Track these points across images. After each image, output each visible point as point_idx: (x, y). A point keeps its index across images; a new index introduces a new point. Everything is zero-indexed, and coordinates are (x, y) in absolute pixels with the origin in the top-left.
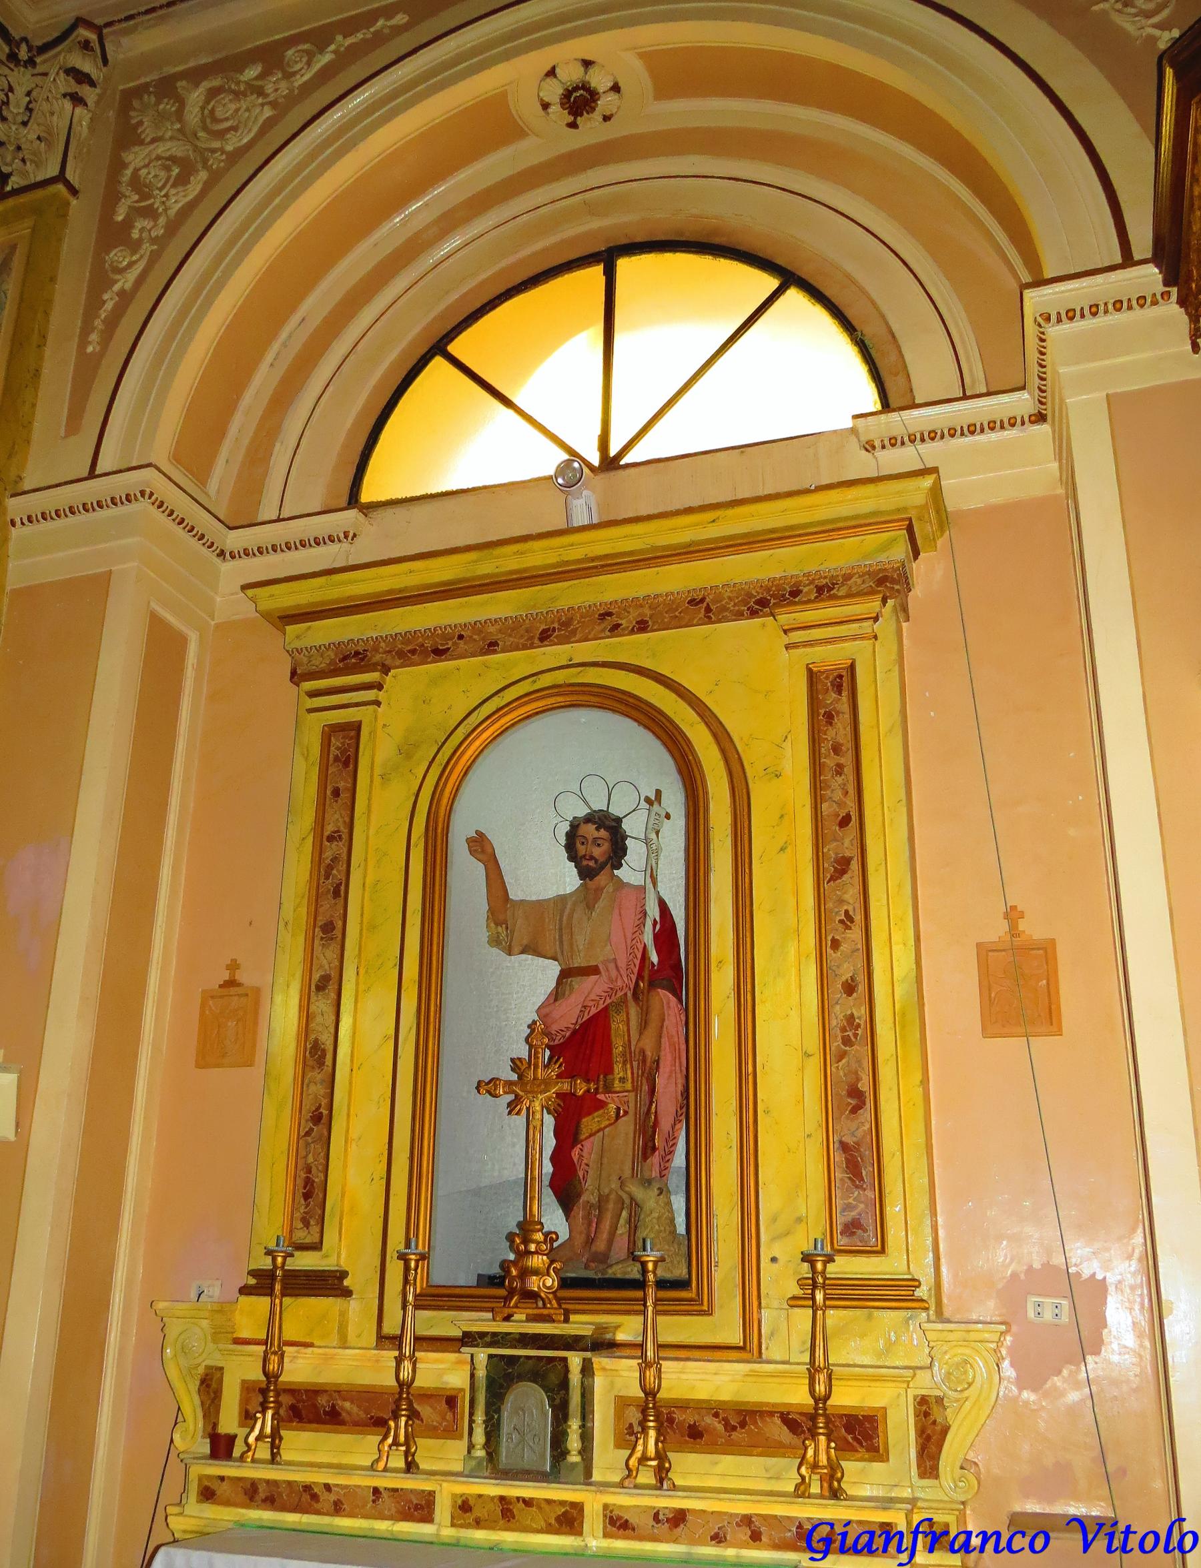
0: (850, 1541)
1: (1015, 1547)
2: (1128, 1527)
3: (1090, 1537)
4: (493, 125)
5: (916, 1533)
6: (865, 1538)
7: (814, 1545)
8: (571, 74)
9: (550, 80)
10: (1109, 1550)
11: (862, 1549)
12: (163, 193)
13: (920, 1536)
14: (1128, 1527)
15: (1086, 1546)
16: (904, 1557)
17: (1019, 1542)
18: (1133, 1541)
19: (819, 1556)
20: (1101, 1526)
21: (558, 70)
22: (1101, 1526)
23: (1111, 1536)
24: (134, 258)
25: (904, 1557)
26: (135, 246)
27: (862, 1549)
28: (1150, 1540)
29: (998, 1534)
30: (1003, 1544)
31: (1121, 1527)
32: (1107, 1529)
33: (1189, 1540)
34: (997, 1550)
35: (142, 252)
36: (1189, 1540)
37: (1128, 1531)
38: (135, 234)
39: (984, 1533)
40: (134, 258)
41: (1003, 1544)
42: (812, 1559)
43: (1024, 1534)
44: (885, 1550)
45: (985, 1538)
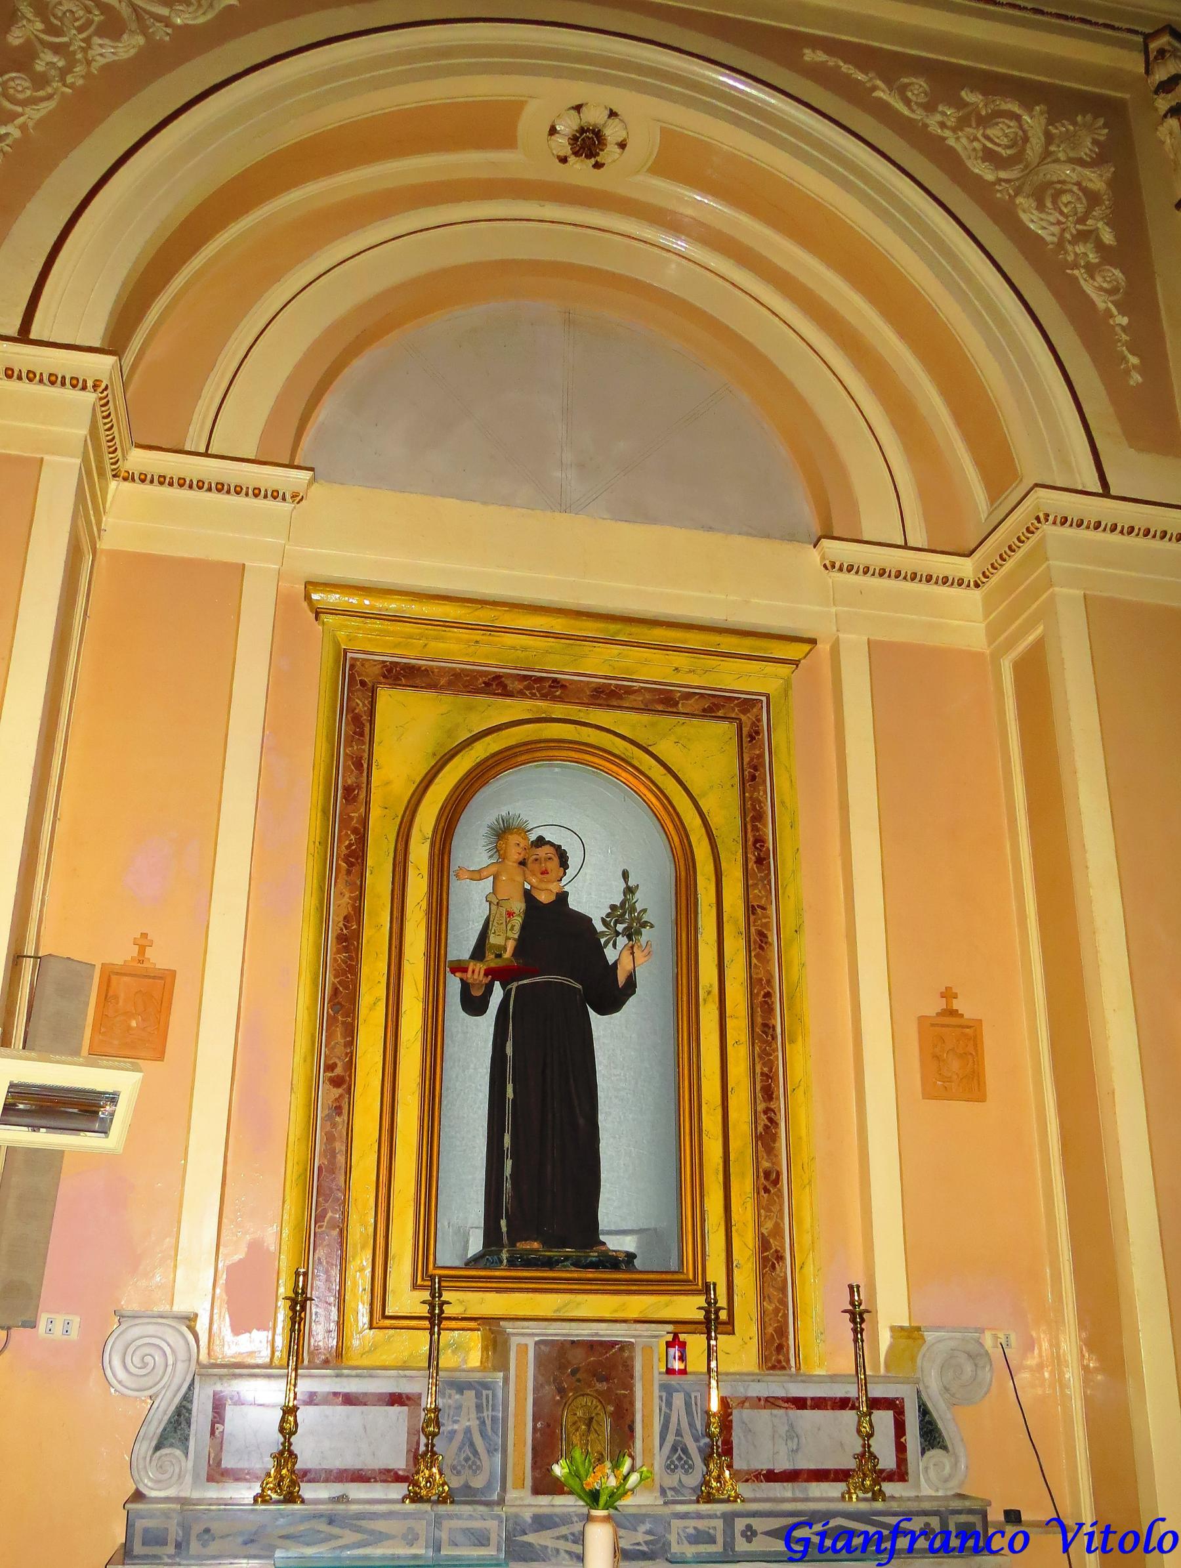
1: (994, 1547)
2: (1108, 1527)
3: (1070, 1536)
4: (493, 126)
10: (1089, 1551)
14: (1108, 1527)
18: (1113, 1541)
22: (1081, 1525)
24: (41, 93)
27: (841, 1549)
28: (1129, 1542)
32: (1087, 1529)
33: (1168, 1542)
35: (49, 90)
36: (1168, 1542)
38: (40, 67)
40: (41, 93)
43: (1003, 1534)
44: (864, 1550)
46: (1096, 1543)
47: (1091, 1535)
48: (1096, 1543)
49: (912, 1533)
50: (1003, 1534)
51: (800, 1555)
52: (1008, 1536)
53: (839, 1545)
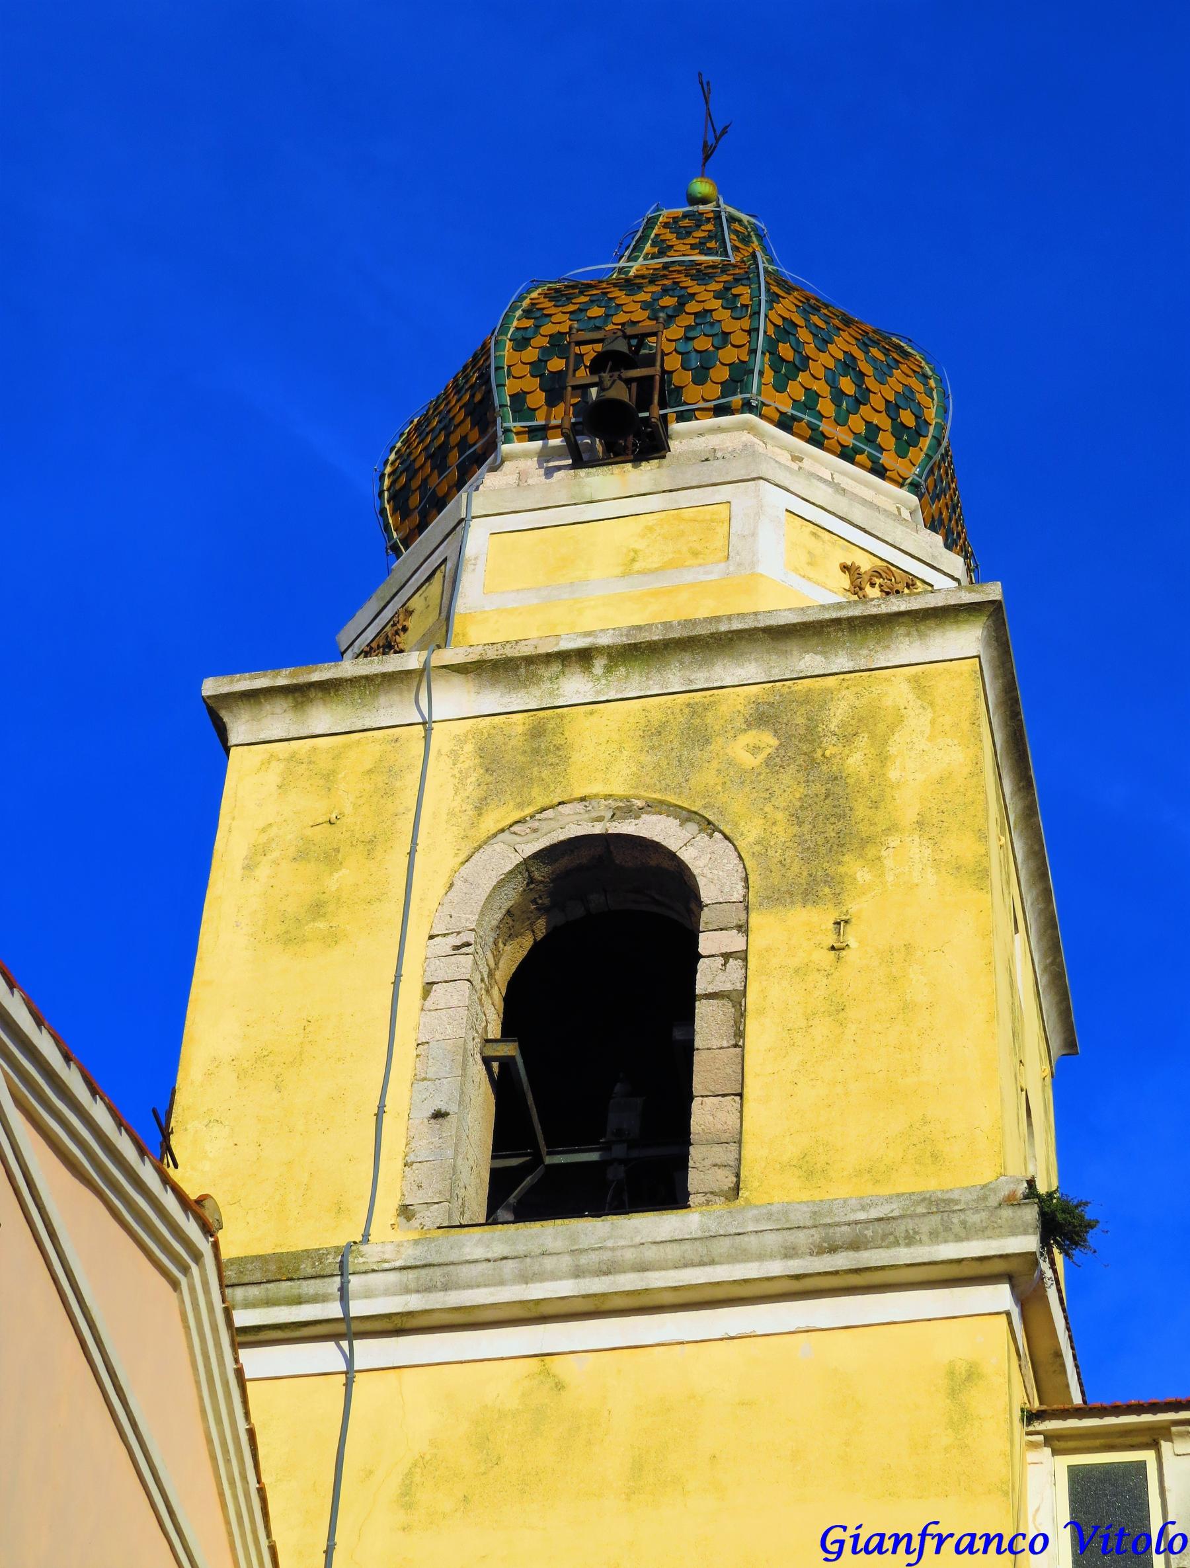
0: (861, 1545)
2: (1122, 1530)
3: (1086, 1540)
5: (923, 1535)
6: (876, 1540)
7: (829, 1547)
11: (873, 1551)
13: (928, 1538)
14: (1122, 1530)
16: (913, 1558)
19: (834, 1556)
20: (1096, 1528)
22: (1096, 1528)
23: (1106, 1538)
25: (913, 1558)
29: (1000, 1536)
30: (1005, 1545)
31: (1115, 1530)
33: (1178, 1543)
34: (999, 1551)
36: (1178, 1543)
37: (1121, 1534)
39: (987, 1535)
41: (1005, 1545)
42: (826, 1559)
45: (988, 1539)
46: (1112, 1543)
47: (1106, 1538)
48: (1112, 1543)
49: (940, 1535)
50: (1024, 1536)
51: (834, 1556)
52: (1029, 1538)
53: (871, 1546)
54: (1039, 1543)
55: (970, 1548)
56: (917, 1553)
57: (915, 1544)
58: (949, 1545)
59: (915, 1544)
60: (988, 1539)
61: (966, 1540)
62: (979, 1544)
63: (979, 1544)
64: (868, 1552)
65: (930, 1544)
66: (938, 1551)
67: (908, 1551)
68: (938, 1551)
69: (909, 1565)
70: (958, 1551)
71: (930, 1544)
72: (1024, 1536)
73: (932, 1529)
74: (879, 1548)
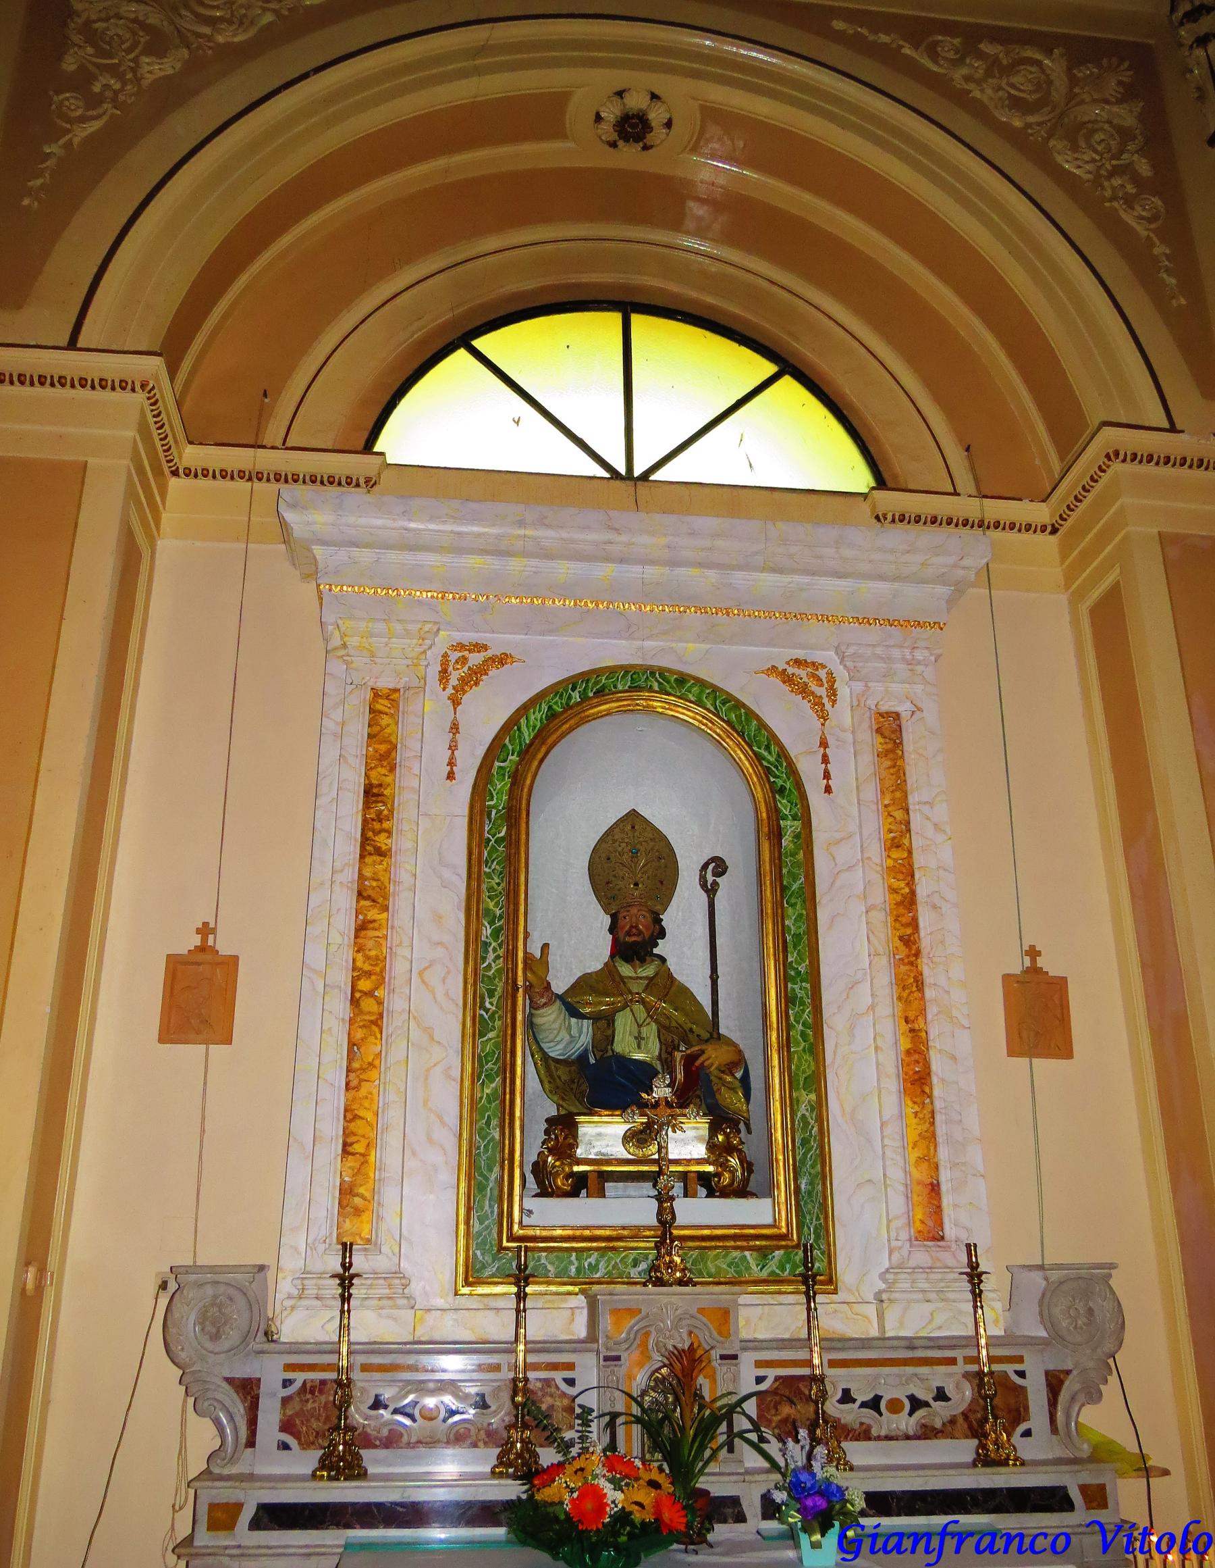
1: (1038, 1547)
3: (1109, 1538)
8: (637, 101)
9: (616, 99)
11: (891, 1551)
12: (132, 56)
13: (948, 1538)
15: (1106, 1547)
16: (932, 1558)
17: (1041, 1543)
19: (849, 1557)
21: (626, 95)
24: (90, 113)
25: (932, 1558)
26: (93, 101)
29: (1021, 1536)
34: (1020, 1551)
35: (100, 111)
40: (90, 113)
47: (1130, 1536)
54: (1061, 1541)
55: (991, 1548)
56: (936, 1553)
57: (935, 1543)
58: (970, 1543)
59: (935, 1543)
60: (1009, 1538)
61: (987, 1540)
62: (1000, 1543)
63: (1000, 1543)
64: (886, 1552)
65: (950, 1543)
66: (957, 1551)
67: (927, 1551)
68: (957, 1551)
69: (928, 1565)
70: (978, 1551)
71: (950, 1543)
72: (1045, 1535)
73: (949, 1529)
74: (898, 1548)
